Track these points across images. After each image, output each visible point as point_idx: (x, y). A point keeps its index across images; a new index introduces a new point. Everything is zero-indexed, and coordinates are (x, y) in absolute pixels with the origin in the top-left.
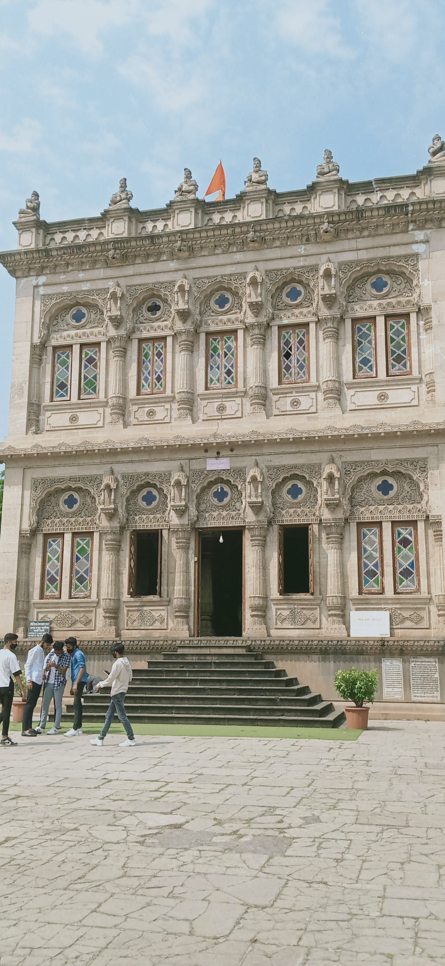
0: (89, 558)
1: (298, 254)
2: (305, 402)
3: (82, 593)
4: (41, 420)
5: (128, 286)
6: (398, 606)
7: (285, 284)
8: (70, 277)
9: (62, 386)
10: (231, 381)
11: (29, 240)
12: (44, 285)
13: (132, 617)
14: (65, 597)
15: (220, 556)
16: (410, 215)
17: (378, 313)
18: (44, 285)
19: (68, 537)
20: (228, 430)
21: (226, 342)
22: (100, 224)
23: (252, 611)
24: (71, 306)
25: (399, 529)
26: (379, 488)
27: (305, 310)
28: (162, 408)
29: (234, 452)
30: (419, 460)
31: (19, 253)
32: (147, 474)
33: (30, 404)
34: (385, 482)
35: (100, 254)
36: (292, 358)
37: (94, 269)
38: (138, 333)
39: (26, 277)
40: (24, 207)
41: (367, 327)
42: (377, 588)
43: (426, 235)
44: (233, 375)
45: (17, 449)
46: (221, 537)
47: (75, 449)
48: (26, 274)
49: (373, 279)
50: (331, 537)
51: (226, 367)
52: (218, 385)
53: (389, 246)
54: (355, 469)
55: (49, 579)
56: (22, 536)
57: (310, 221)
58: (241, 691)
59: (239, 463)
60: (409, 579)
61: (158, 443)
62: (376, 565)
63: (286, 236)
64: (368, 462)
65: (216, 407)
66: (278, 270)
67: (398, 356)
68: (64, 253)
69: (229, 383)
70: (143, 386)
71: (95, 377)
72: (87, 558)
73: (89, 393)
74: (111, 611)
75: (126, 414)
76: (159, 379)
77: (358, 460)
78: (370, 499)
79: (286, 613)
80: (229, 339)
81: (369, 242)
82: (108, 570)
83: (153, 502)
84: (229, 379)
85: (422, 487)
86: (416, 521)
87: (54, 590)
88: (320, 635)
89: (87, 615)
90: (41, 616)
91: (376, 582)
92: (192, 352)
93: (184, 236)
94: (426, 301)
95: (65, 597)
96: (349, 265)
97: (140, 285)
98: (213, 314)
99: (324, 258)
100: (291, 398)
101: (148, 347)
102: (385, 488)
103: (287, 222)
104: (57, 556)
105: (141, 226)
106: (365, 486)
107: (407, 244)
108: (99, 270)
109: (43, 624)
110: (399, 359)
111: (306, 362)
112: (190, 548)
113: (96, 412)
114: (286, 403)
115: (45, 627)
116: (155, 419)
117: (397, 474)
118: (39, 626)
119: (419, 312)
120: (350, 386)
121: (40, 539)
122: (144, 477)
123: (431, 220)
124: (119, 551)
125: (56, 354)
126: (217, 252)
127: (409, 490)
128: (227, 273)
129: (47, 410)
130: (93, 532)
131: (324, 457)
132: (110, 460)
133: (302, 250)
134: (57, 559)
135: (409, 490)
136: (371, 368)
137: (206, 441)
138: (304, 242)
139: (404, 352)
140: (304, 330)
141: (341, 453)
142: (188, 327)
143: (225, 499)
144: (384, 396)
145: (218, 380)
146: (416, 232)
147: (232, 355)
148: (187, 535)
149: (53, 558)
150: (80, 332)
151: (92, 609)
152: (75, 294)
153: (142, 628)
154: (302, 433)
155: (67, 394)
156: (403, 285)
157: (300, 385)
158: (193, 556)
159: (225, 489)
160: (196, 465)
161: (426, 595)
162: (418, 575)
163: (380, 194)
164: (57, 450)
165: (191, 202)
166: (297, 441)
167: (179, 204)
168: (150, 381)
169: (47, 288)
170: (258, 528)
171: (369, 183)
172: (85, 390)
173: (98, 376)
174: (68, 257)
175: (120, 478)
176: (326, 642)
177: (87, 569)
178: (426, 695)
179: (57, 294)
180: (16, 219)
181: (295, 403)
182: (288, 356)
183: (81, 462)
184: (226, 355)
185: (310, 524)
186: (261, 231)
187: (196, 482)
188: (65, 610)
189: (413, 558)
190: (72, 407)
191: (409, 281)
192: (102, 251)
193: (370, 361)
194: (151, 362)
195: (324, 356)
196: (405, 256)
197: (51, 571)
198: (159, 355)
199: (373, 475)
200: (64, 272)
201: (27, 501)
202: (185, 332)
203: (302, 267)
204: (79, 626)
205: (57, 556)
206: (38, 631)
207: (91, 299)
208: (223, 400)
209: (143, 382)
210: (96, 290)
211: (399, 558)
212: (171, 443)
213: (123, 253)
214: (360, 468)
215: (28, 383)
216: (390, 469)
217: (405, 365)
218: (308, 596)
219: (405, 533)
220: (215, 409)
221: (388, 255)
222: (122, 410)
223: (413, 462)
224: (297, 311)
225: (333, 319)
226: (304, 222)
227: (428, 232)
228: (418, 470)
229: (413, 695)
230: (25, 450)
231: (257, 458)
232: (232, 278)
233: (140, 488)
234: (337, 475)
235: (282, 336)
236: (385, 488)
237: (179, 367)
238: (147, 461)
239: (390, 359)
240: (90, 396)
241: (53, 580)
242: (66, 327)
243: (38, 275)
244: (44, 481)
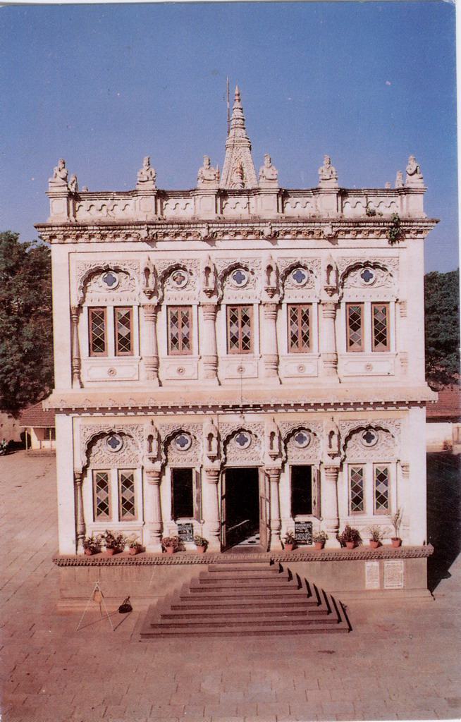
15: (242, 491)
82: (154, 499)
127: (385, 439)
229: (385, 585)
236: (368, 438)
242: (99, 289)
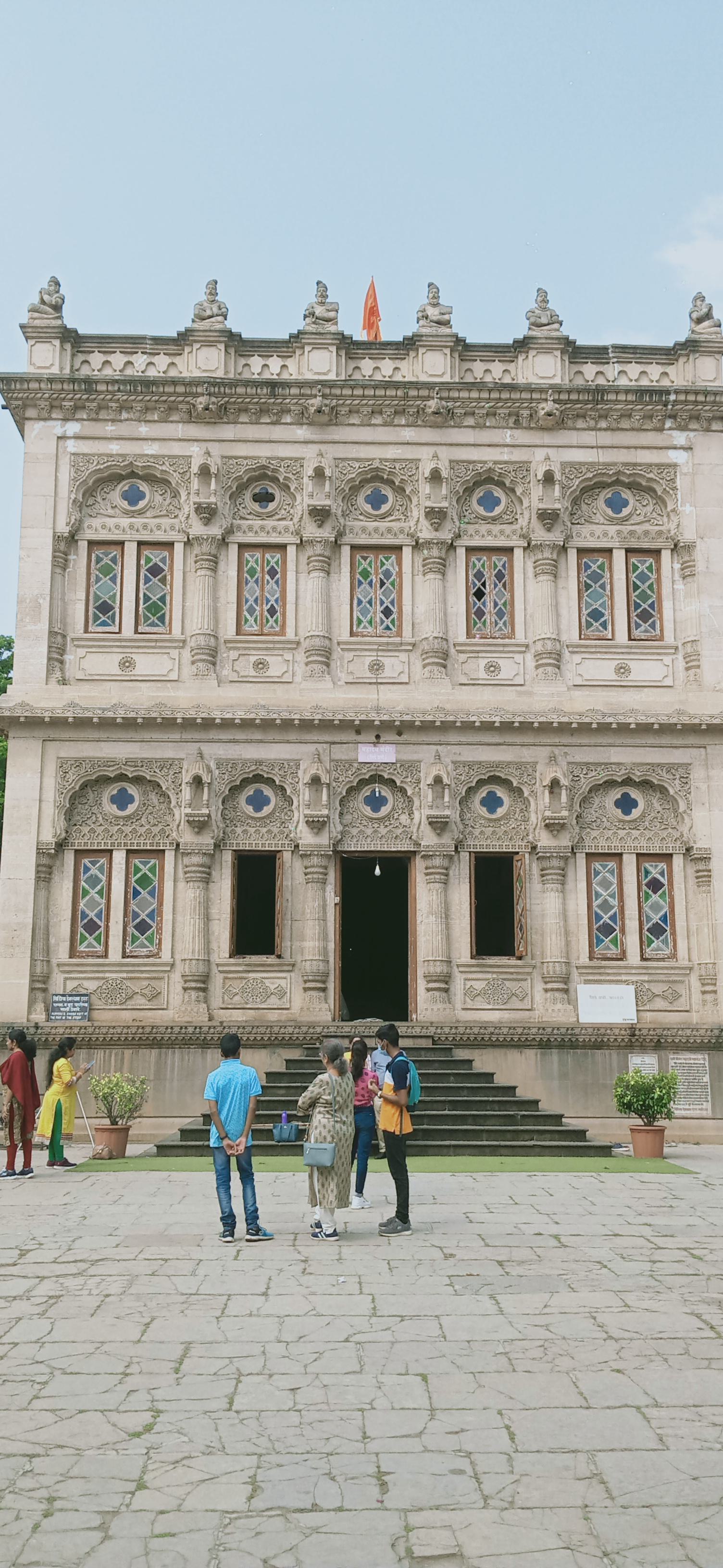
0: (157, 894)
1: (501, 442)
2: (508, 669)
3: (145, 950)
4: (68, 661)
5: (226, 457)
6: (646, 978)
7: (477, 484)
8: (124, 429)
9: (105, 608)
10: (391, 626)
11: (48, 359)
12: (77, 437)
13: (231, 989)
14: (115, 954)
15: (374, 896)
16: (670, 407)
17: (617, 545)
18: (77, 437)
19: (119, 857)
20: (396, 702)
21: (383, 564)
22: (172, 348)
23: (428, 982)
24: (120, 478)
25: (647, 865)
26: (618, 804)
27: (508, 529)
28: (280, 658)
29: (405, 737)
30: (680, 765)
31: (39, 380)
32: (259, 762)
33: (52, 633)
34: (626, 796)
35: (181, 399)
36: (487, 598)
37: (166, 422)
38: (239, 534)
39: (45, 419)
40: (36, 300)
41: (599, 563)
42: (614, 951)
43: (688, 438)
44: (394, 616)
45: (37, 708)
46: (378, 868)
47: (143, 713)
48: (45, 414)
49: (607, 493)
50: (547, 875)
51: (382, 603)
52: (370, 629)
53: (636, 448)
54: (586, 774)
55: (88, 926)
56: (40, 852)
57: (525, 395)
58: (455, 1105)
59: (409, 754)
60: (661, 938)
61: (285, 715)
62: (613, 918)
63: (485, 412)
64: (606, 764)
65: (368, 663)
66: (470, 462)
67: (645, 612)
68: (119, 390)
69: (388, 628)
70: (246, 620)
71: (163, 599)
72: (152, 893)
73: (153, 625)
74: (199, 978)
75: (218, 662)
76: (272, 611)
77: (591, 761)
78: (604, 819)
79: (479, 986)
80: (387, 559)
81: (606, 438)
82: (196, 914)
83: (265, 808)
84: (387, 622)
85: (682, 807)
86: (671, 855)
87: (95, 943)
88: (532, 1020)
89: (153, 983)
90: (71, 985)
91: (614, 941)
92: (328, 573)
93: (327, 391)
94: (688, 535)
95: (115, 954)
96: (570, 467)
97: (246, 458)
98: (361, 517)
99: (540, 454)
100: (486, 661)
101: (252, 558)
102: (626, 804)
103: (490, 391)
104: (99, 887)
105: (243, 361)
106: (597, 800)
107: (661, 448)
108: (174, 425)
109: (78, 999)
110: (645, 616)
111: (508, 607)
112: (327, 882)
113: (165, 656)
114: (478, 668)
115: (82, 1004)
116: (267, 674)
117: (645, 785)
118: (70, 1002)
119: (675, 549)
120: (574, 649)
121: (69, 858)
122: (254, 767)
123: (697, 418)
124: (207, 883)
125: (93, 555)
126: (374, 421)
127: (660, 809)
128: (388, 457)
129: (78, 646)
130: (164, 851)
131: (542, 753)
132: (197, 736)
133: (508, 436)
134: (100, 893)
135: (660, 809)
136: (604, 625)
137: (363, 717)
138: (511, 425)
139: (652, 606)
140: (505, 559)
141: (566, 749)
142: (326, 535)
143: (383, 809)
144: (624, 668)
145: (370, 623)
146: (675, 433)
147: (393, 584)
148: (324, 862)
149: (91, 891)
150: (138, 521)
151: (161, 975)
152: (131, 459)
153: (248, 1006)
154: (514, 715)
155: (114, 622)
156: (650, 508)
157: (500, 641)
158: (333, 894)
159: (383, 793)
160: (340, 753)
161: (686, 963)
162: (674, 933)
163: (618, 367)
164: (110, 714)
165: (332, 337)
166: (507, 727)
167: (313, 336)
168: (257, 613)
169: (81, 442)
170: (439, 855)
171: (604, 349)
172: (147, 618)
173: (168, 598)
175: (213, 765)
176: (550, 1030)
177: (153, 910)
178: (691, 1107)
179: (100, 455)
180: (25, 321)
181: (492, 668)
182: (479, 594)
183: (147, 735)
184: (382, 584)
185: (517, 853)
186: (448, 399)
187: (340, 780)
188: (114, 975)
189: (666, 909)
190: (123, 644)
191: (661, 501)
192: (186, 395)
193: (603, 615)
194: (260, 583)
195: (542, 602)
196: (659, 466)
197: (87, 911)
198: (272, 573)
199: (610, 784)
200: (113, 421)
201: (50, 794)
202: (320, 542)
203: (506, 463)
204: (140, 1001)
205: (99, 887)
206: (68, 1009)
207: (160, 469)
208: (380, 653)
209: (246, 613)
210: (169, 457)
211: (646, 909)
212: (307, 716)
213: (225, 402)
214: (594, 773)
215: (48, 599)
216: (637, 776)
217: (653, 626)
218: (513, 961)
219: (655, 870)
220: (367, 667)
221: (634, 461)
222: (211, 656)
223: (670, 768)
224: (496, 528)
225: (554, 547)
226: (516, 395)
227: (692, 434)
228: (677, 782)
230: (52, 710)
231: (439, 747)
232: (398, 466)
233: (246, 782)
234: (564, 782)
235: (471, 564)
237: (313, 598)
238: (261, 741)
239: (633, 615)
240: (155, 629)
241: (92, 927)
242: (110, 512)
243: (65, 420)
244: (78, 763)
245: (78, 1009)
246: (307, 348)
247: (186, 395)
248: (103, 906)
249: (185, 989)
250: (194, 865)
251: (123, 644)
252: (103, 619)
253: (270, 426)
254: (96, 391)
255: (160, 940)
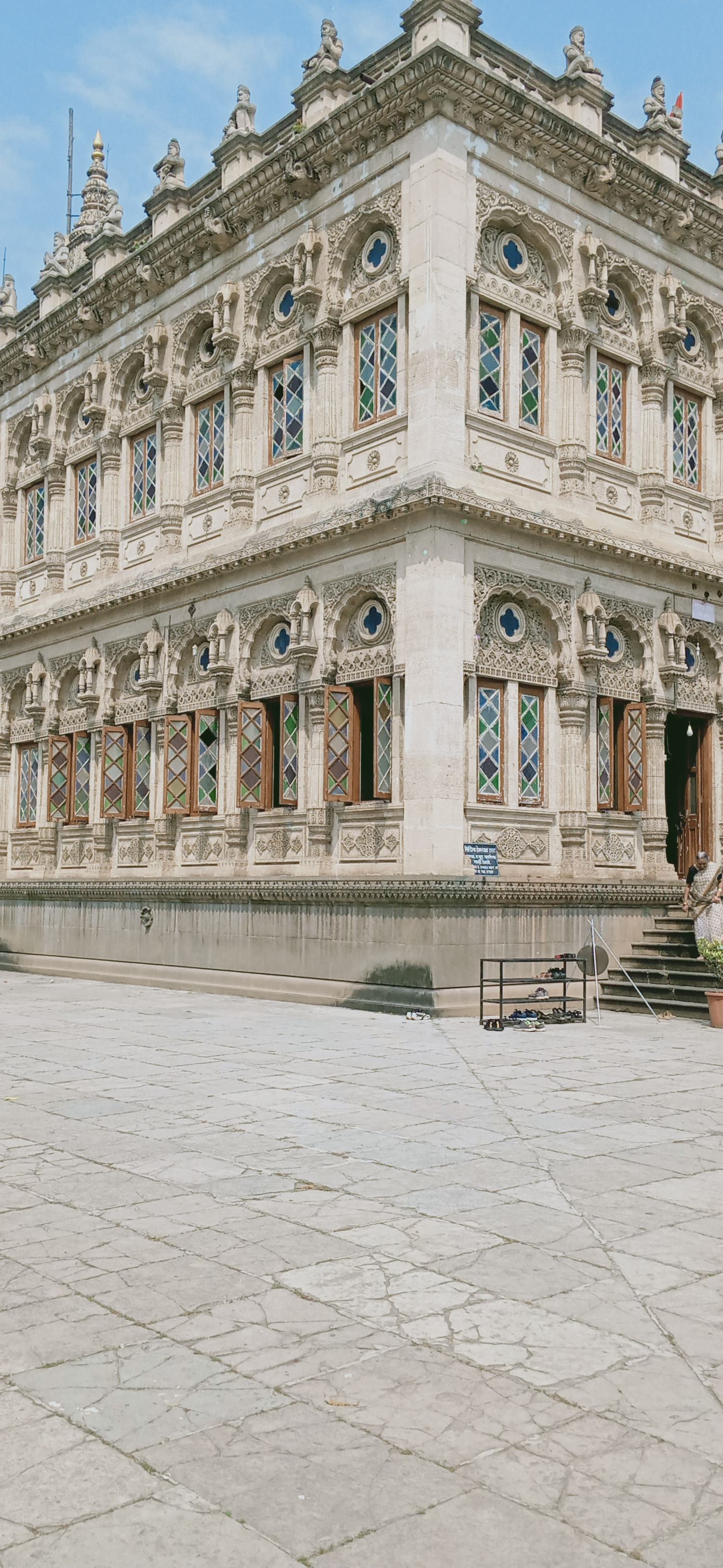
18: (484, 161)
19: (512, 689)
32: (625, 603)
35: (585, 159)
87: (493, 787)
104: (494, 722)
109: (486, 850)
130: (547, 688)
132: (587, 563)
153: (610, 864)
169: (486, 169)
174: (542, 134)
190: (508, 436)
192: (592, 157)
205: (494, 722)
230: (494, 503)
238: (630, 581)
245: (488, 862)
246: (660, 149)
247: (592, 157)
248: (498, 744)
249: (564, 844)
250: (579, 709)
251: (508, 436)
252: (488, 399)
253: (635, 224)
254: (521, 114)
255: (543, 787)
